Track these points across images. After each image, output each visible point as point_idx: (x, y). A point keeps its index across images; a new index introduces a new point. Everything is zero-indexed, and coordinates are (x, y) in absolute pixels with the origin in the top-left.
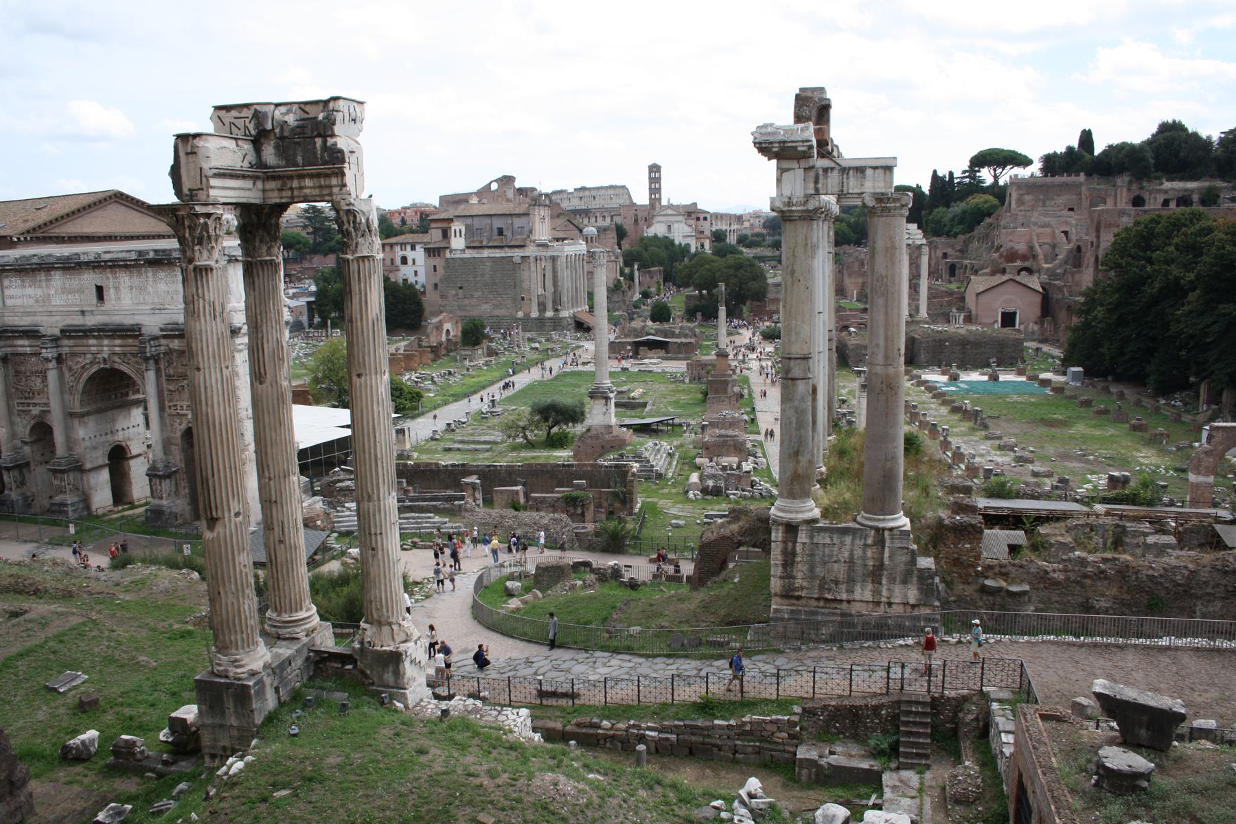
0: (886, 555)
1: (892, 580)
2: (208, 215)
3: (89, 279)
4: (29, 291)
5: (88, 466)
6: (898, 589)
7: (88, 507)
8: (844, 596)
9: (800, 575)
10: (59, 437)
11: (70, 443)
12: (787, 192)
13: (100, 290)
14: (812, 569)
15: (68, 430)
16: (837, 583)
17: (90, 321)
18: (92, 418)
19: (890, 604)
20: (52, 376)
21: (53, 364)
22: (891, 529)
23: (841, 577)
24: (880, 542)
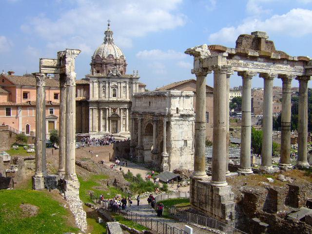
0: (214, 196)
1: (215, 207)
2: (39, 76)
3: (148, 100)
4: (139, 103)
5: (145, 149)
6: (217, 209)
7: (143, 160)
8: (204, 209)
9: (195, 197)
10: (139, 140)
11: (142, 142)
12: (196, 68)
13: (150, 102)
14: (198, 196)
15: (142, 139)
16: (203, 203)
17: (147, 110)
18: (148, 136)
19: (215, 216)
20: (139, 124)
21: (140, 121)
22: (215, 186)
23: (204, 201)
24: (212, 191)
